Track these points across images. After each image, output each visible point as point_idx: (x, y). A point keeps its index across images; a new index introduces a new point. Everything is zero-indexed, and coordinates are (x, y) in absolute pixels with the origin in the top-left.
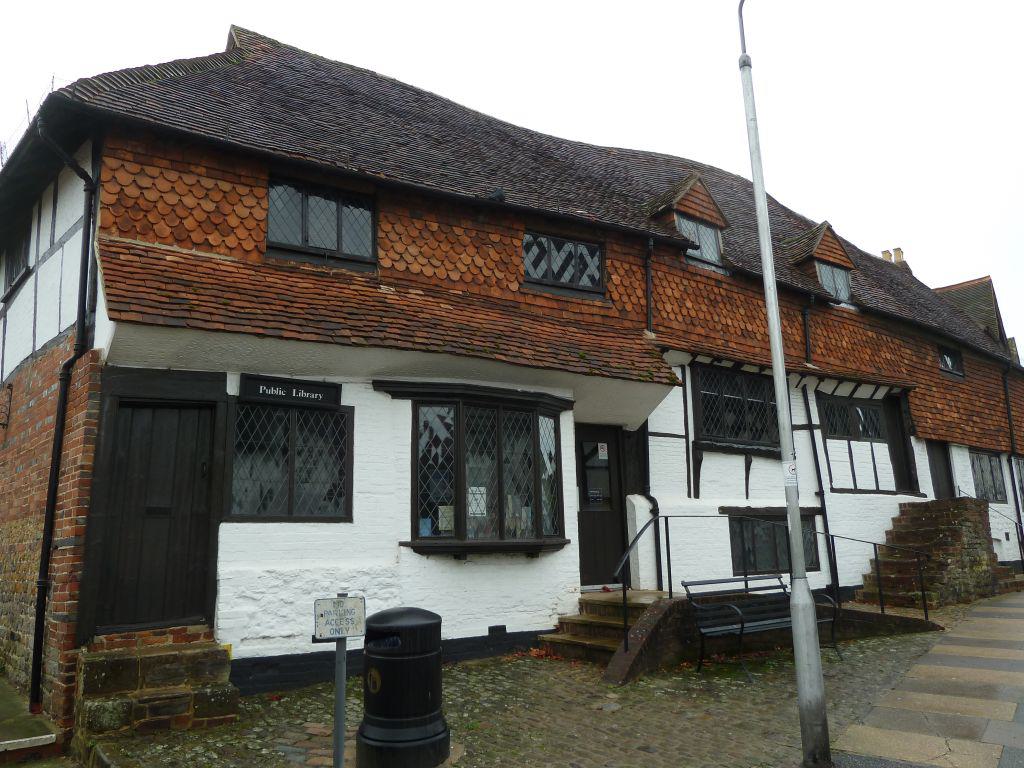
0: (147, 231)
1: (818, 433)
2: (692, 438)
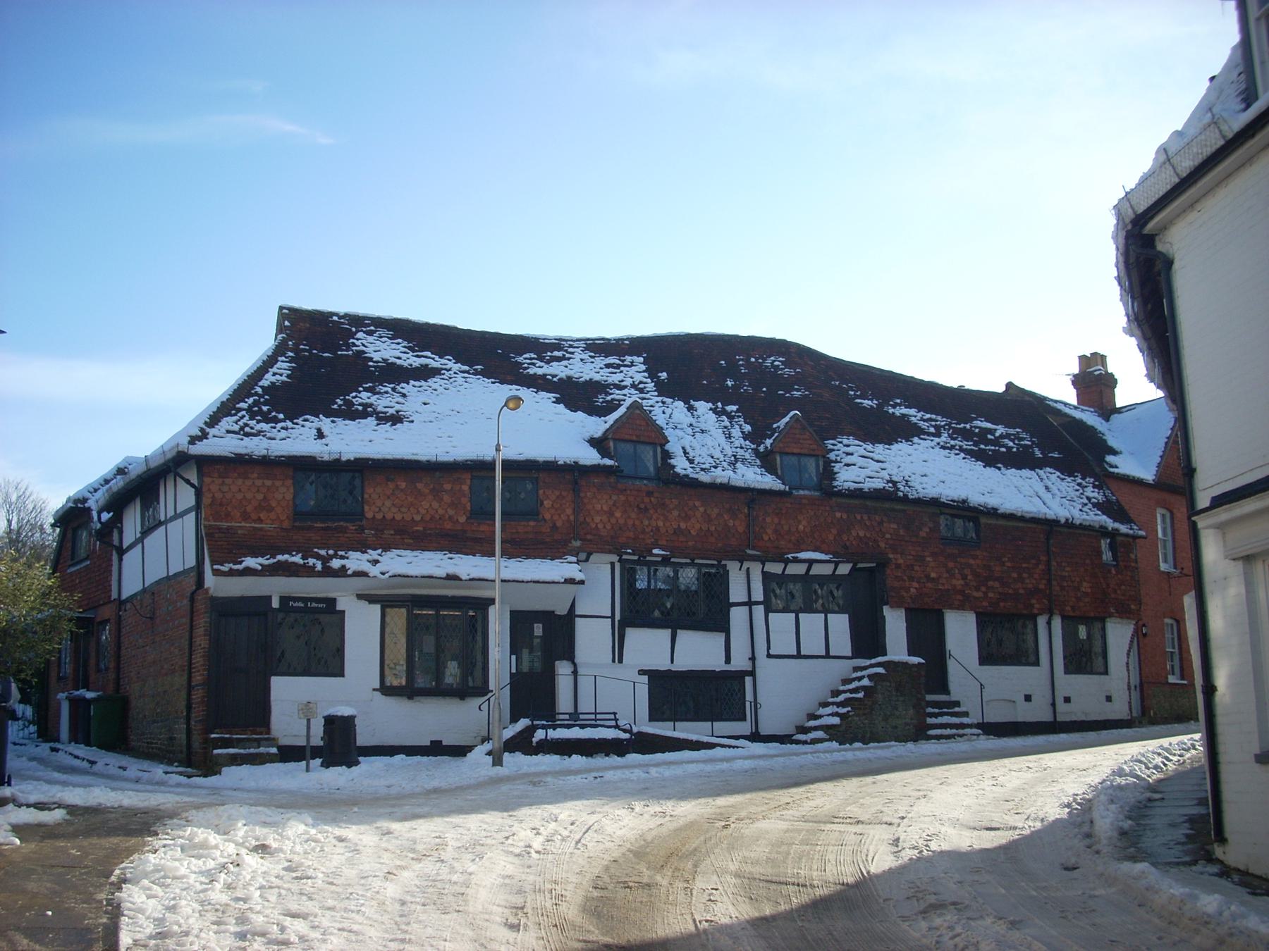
0: (228, 516)
1: (759, 611)
2: (618, 617)
